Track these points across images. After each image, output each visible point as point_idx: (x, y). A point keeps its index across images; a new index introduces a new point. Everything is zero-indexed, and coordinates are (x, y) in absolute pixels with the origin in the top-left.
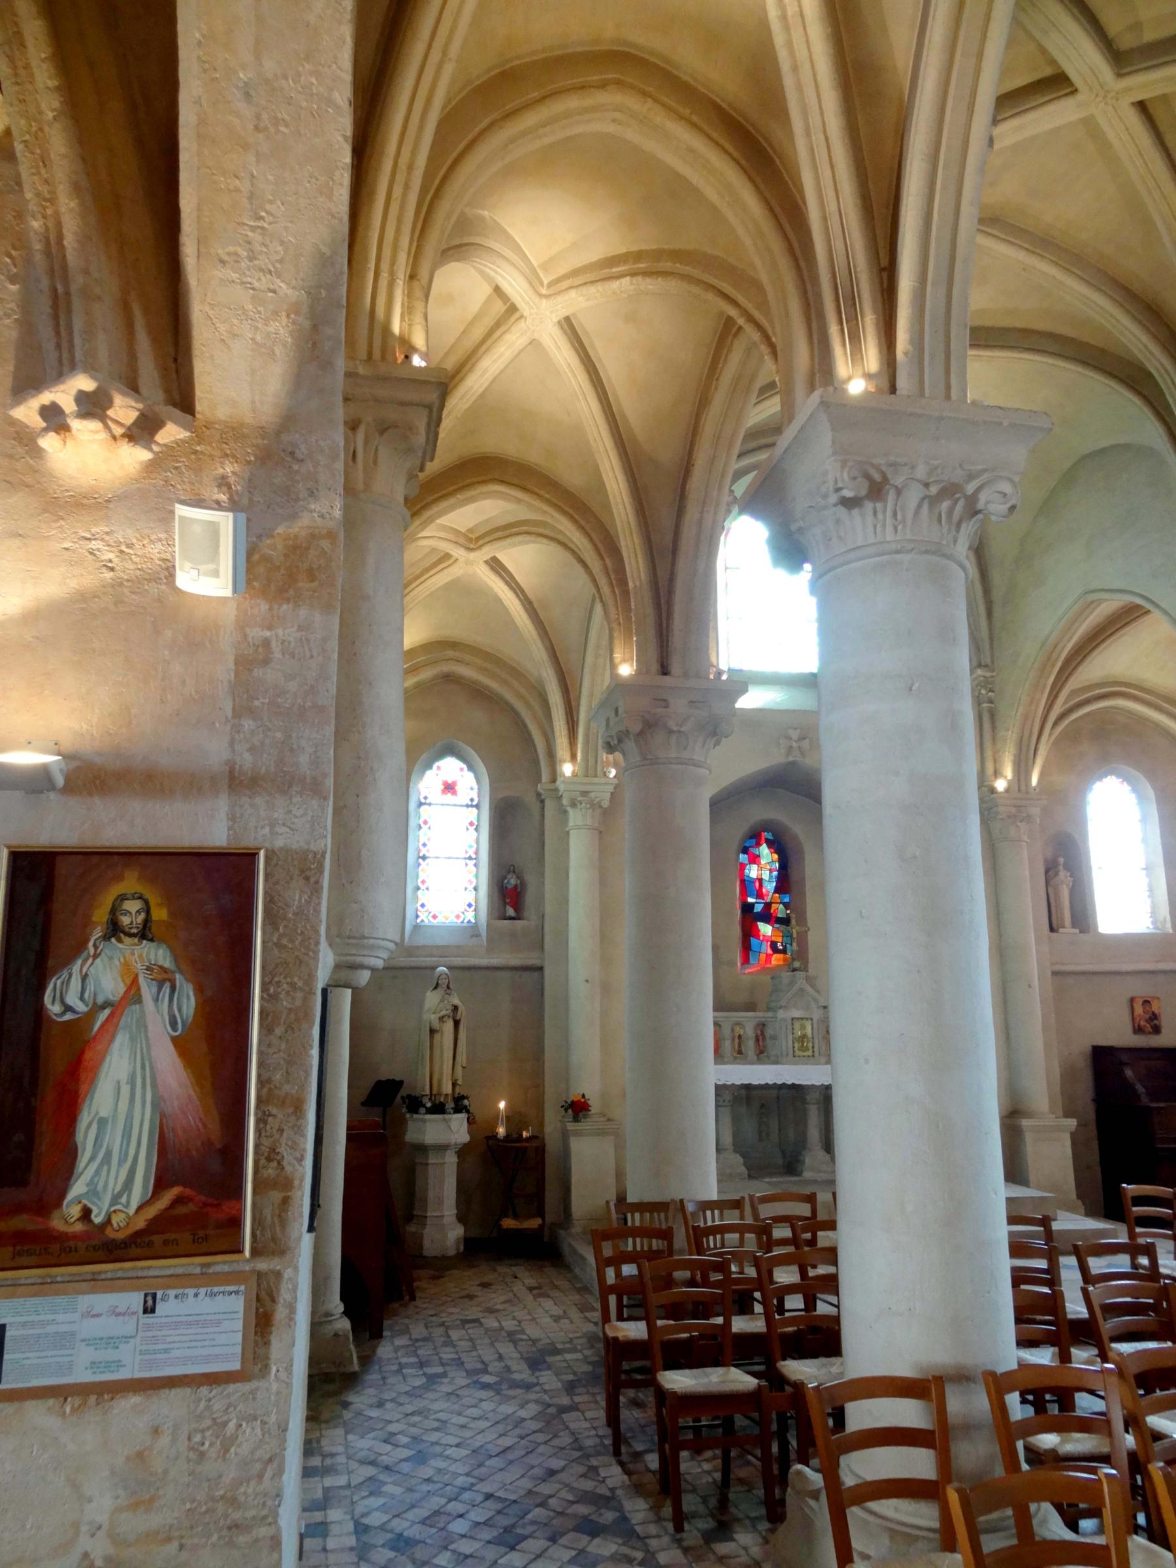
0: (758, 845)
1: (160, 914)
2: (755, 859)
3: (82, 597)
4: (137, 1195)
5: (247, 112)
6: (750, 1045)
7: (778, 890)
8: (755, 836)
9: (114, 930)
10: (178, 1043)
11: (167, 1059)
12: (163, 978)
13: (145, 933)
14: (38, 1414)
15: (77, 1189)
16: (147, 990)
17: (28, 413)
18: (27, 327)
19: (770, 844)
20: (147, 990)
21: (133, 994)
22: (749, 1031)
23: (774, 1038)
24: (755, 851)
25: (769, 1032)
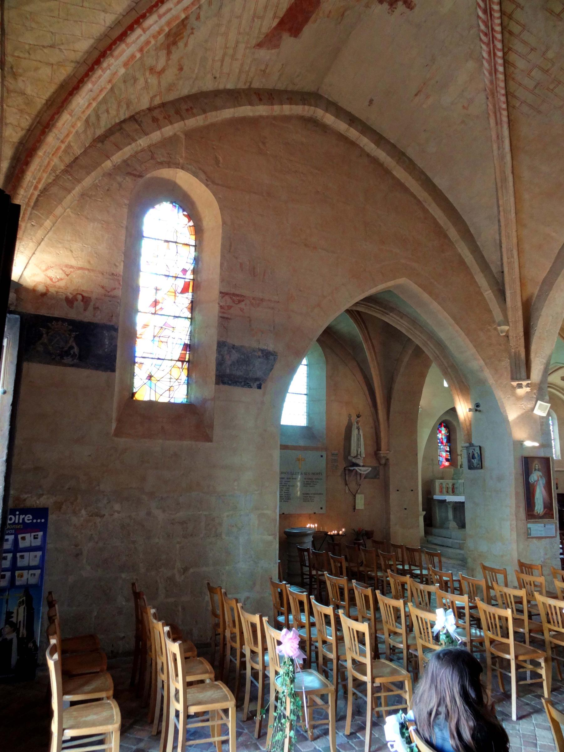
0: (441, 427)
1: (540, 467)
2: (440, 432)
3: (522, 414)
4: (542, 510)
5: (546, 334)
6: (450, 490)
7: (447, 442)
8: (441, 425)
9: (535, 470)
10: (544, 487)
11: (543, 489)
12: (541, 477)
13: (539, 470)
14: (535, 540)
15: (536, 509)
16: (540, 479)
17: (515, 384)
18: (511, 367)
19: (445, 427)
20: (540, 479)
21: (538, 480)
22: (450, 486)
23: (457, 488)
24: (440, 429)
25: (455, 486)
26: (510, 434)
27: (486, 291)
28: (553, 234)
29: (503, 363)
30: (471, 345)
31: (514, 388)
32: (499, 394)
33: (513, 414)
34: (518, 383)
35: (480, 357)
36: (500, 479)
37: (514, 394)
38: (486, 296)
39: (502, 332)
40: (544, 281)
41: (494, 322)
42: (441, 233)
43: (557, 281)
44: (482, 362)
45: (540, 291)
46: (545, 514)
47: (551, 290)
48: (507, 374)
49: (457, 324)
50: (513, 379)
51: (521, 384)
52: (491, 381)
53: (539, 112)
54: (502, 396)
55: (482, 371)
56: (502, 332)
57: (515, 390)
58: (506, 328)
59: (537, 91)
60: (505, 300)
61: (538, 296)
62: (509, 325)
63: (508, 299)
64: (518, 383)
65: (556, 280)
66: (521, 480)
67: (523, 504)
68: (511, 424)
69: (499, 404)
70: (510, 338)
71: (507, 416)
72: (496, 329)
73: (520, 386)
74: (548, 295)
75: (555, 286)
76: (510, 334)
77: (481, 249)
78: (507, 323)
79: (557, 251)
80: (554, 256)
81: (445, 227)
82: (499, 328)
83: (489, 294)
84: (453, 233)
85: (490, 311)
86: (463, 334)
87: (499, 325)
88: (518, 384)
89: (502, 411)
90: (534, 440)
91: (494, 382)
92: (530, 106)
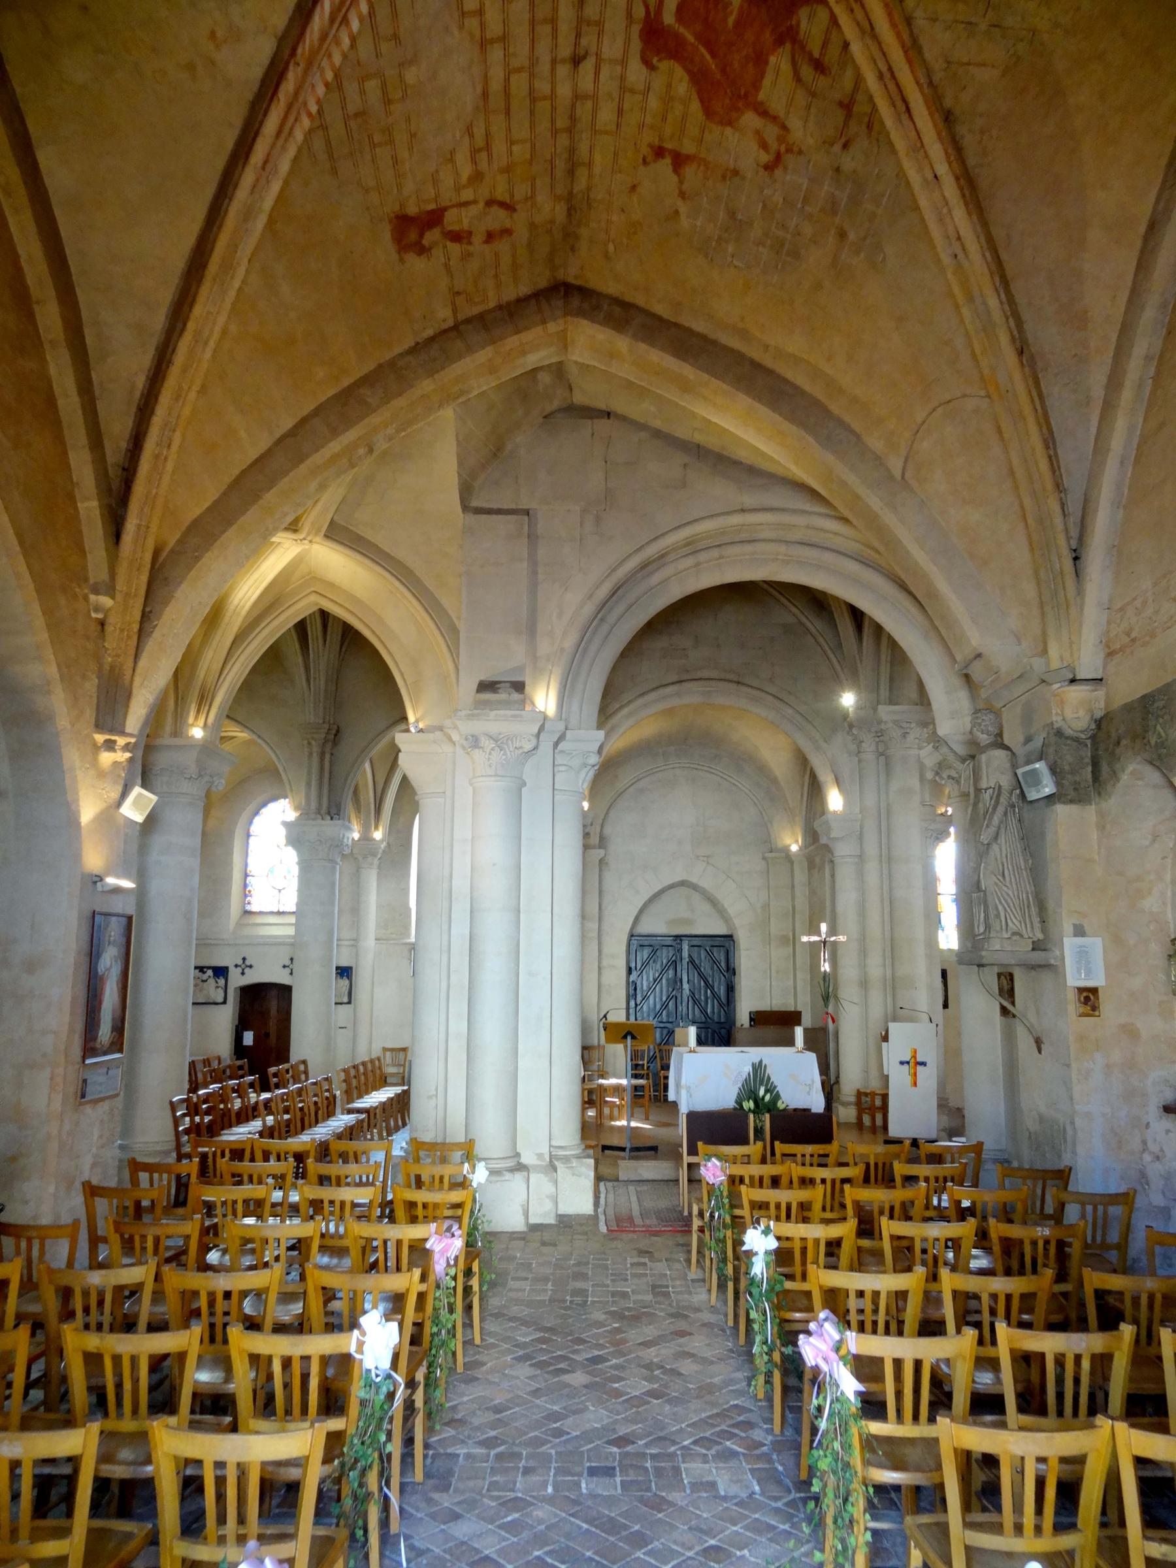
17: (100, 738)
18: (98, 697)
26: (76, 857)
27: (87, 499)
28: (243, 434)
29: (88, 685)
30: (40, 622)
31: (96, 749)
32: (72, 756)
33: (87, 812)
34: (108, 737)
35: (52, 657)
36: (32, 966)
37: (95, 762)
38: (81, 512)
39: (97, 609)
40: (195, 524)
41: (86, 579)
42: (23, 301)
43: (224, 536)
44: (53, 671)
45: (180, 541)
46: (112, 1043)
47: (207, 550)
48: (90, 714)
49: (26, 554)
50: (99, 727)
51: (115, 742)
52: (63, 721)
53: (334, 171)
54: (78, 764)
55: (49, 692)
56: (97, 609)
57: (97, 754)
58: (106, 601)
59: (353, 124)
60: (118, 536)
61: (172, 551)
62: (113, 598)
63: (128, 537)
64: (108, 737)
65: (224, 532)
66: (84, 968)
67: (80, 1026)
68: (84, 832)
69: (68, 782)
70: (109, 629)
71: (79, 812)
72: (86, 598)
73: (110, 746)
74: (197, 559)
75: (218, 543)
76: (112, 620)
77: (97, 392)
78: (111, 591)
79: (236, 472)
80: (228, 480)
81: (35, 292)
82: (92, 597)
83: (90, 508)
84: (49, 317)
85: (82, 552)
86: (32, 586)
87: (96, 592)
88: (107, 741)
89: (69, 799)
90: (126, 875)
91: (69, 727)
92: (328, 142)
